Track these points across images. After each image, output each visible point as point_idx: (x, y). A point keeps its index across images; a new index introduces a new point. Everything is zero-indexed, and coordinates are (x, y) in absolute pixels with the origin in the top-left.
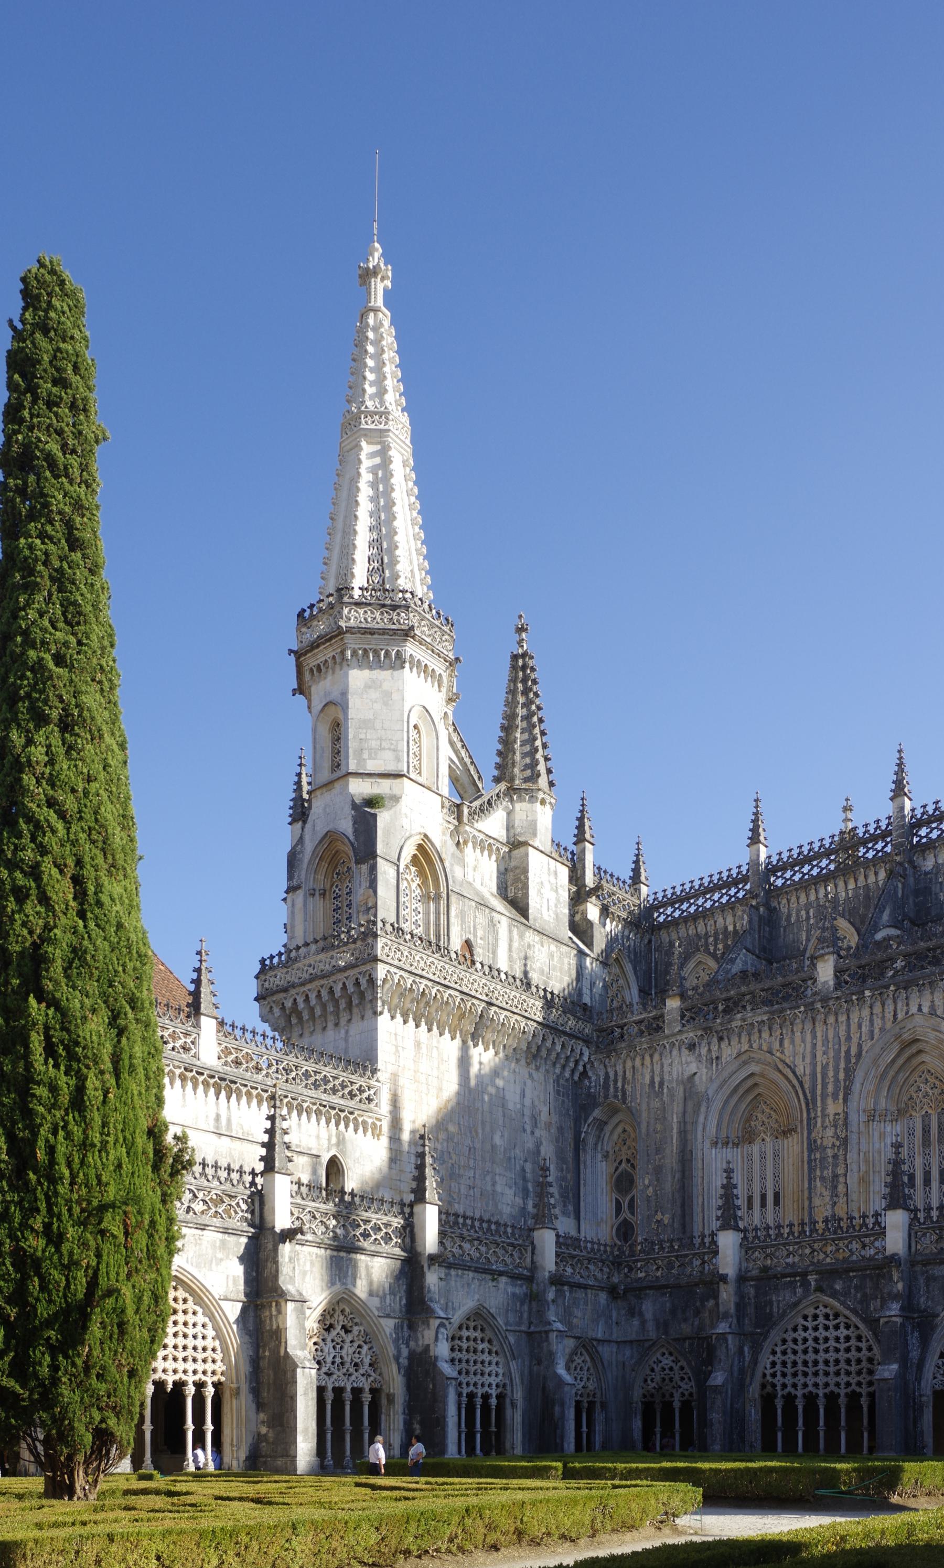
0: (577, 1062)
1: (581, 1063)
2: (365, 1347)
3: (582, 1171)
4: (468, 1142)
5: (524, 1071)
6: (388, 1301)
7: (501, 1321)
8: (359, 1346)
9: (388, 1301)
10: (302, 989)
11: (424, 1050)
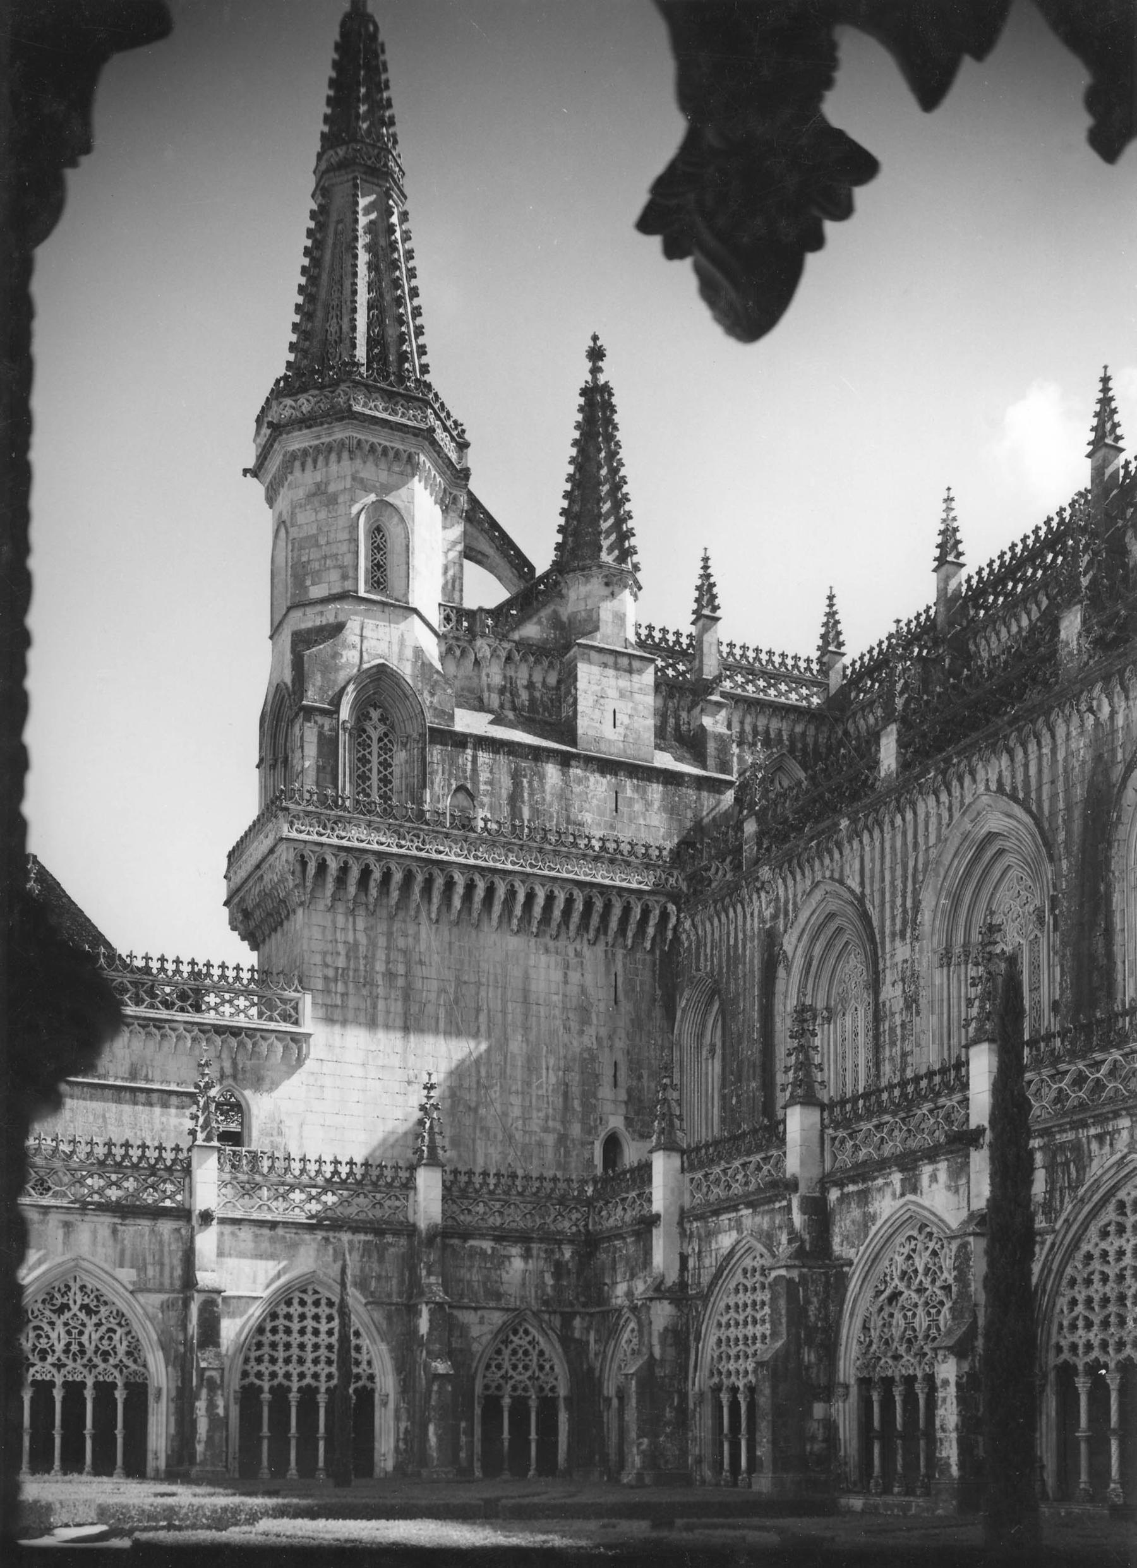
2: (120, 1331)
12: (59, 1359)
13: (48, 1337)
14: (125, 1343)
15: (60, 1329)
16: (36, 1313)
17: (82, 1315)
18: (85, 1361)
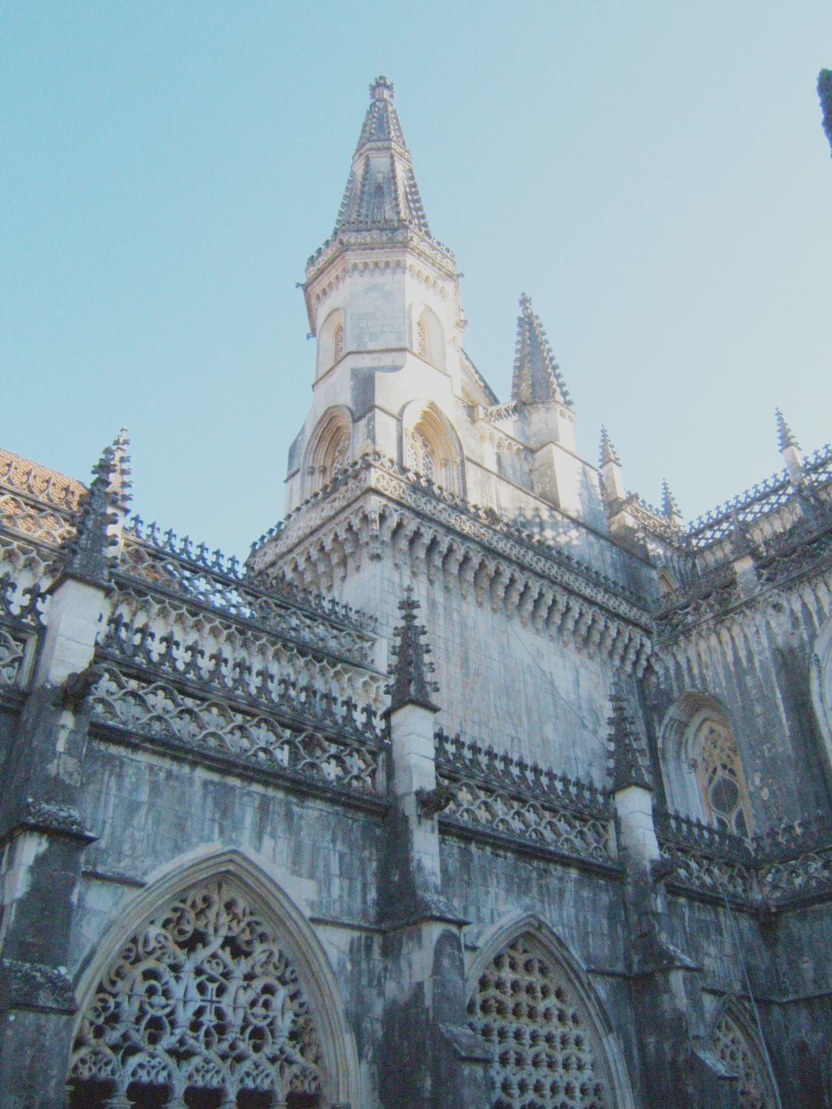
0: (638, 653)
1: (644, 657)
2: (282, 993)
3: (666, 785)
4: (509, 730)
5: (575, 657)
6: (336, 891)
7: (575, 953)
8: (268, 989)
9: (336, 891)
10: (290, 557)
11: (441, 610)
12: (182, 1042)
13: (166, 994)
14: (290, 1016)
15: (189, 980)
16: (153, 944)
17: (226, 955)
18: (225, 1046)
